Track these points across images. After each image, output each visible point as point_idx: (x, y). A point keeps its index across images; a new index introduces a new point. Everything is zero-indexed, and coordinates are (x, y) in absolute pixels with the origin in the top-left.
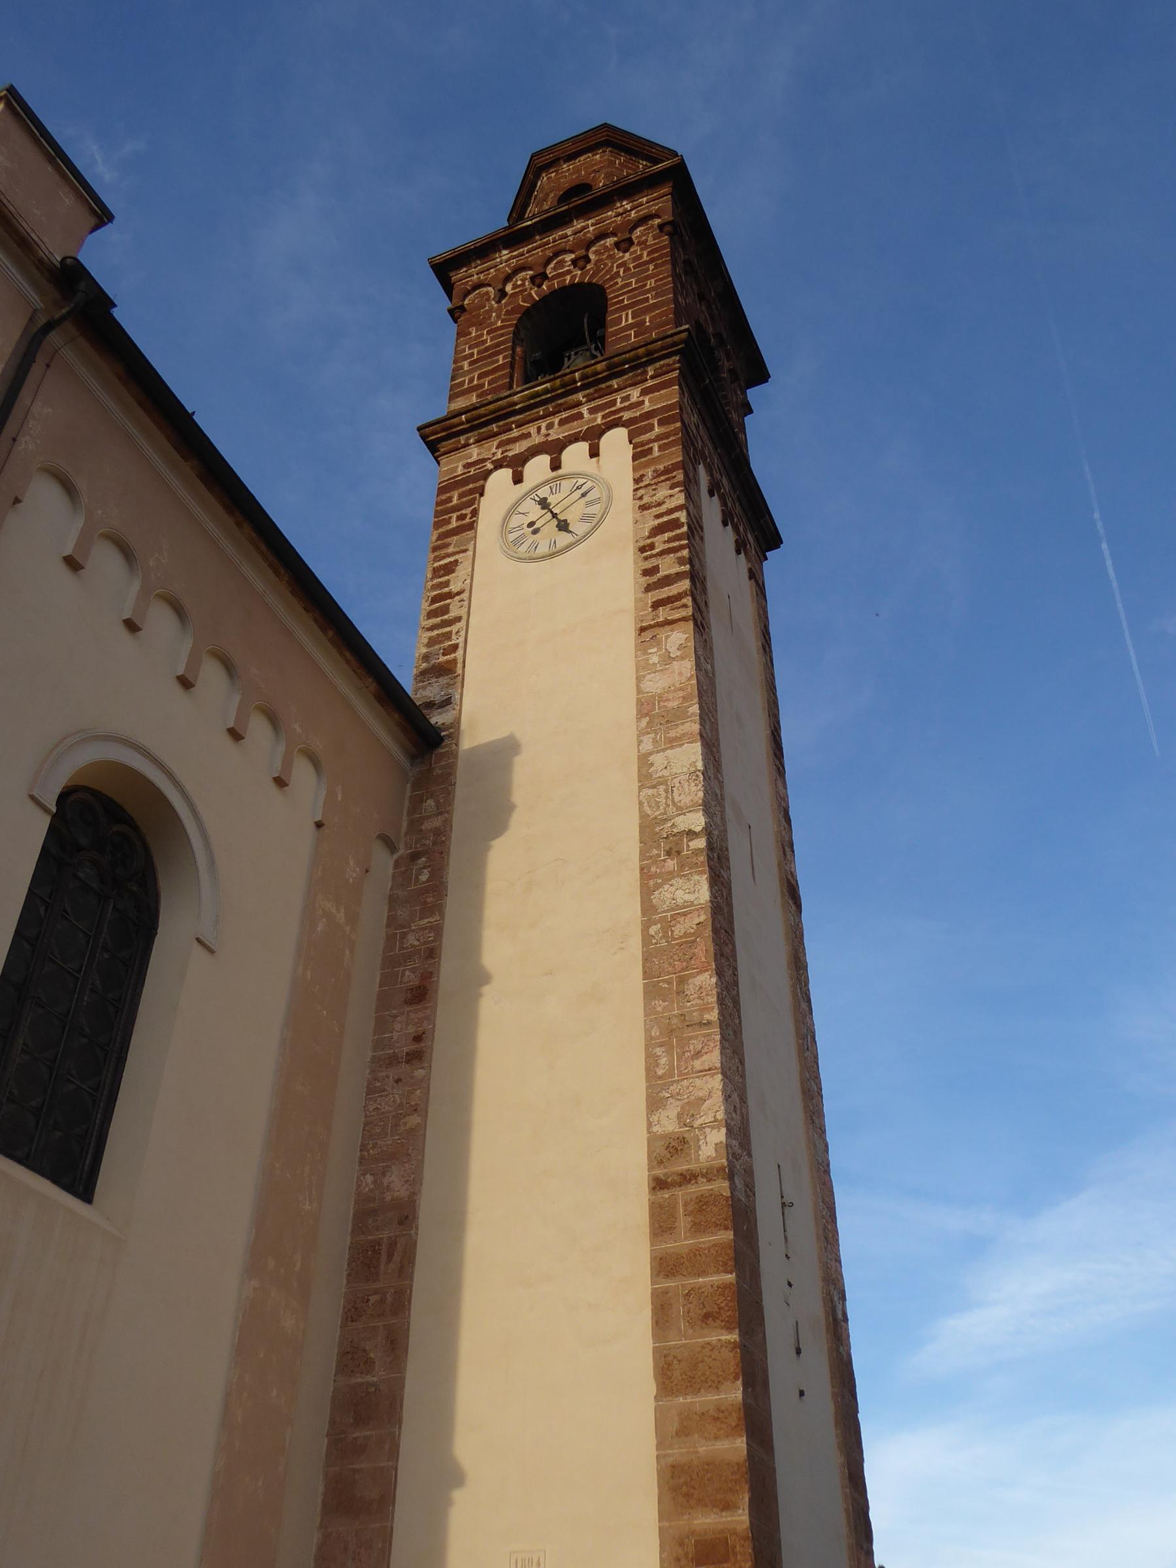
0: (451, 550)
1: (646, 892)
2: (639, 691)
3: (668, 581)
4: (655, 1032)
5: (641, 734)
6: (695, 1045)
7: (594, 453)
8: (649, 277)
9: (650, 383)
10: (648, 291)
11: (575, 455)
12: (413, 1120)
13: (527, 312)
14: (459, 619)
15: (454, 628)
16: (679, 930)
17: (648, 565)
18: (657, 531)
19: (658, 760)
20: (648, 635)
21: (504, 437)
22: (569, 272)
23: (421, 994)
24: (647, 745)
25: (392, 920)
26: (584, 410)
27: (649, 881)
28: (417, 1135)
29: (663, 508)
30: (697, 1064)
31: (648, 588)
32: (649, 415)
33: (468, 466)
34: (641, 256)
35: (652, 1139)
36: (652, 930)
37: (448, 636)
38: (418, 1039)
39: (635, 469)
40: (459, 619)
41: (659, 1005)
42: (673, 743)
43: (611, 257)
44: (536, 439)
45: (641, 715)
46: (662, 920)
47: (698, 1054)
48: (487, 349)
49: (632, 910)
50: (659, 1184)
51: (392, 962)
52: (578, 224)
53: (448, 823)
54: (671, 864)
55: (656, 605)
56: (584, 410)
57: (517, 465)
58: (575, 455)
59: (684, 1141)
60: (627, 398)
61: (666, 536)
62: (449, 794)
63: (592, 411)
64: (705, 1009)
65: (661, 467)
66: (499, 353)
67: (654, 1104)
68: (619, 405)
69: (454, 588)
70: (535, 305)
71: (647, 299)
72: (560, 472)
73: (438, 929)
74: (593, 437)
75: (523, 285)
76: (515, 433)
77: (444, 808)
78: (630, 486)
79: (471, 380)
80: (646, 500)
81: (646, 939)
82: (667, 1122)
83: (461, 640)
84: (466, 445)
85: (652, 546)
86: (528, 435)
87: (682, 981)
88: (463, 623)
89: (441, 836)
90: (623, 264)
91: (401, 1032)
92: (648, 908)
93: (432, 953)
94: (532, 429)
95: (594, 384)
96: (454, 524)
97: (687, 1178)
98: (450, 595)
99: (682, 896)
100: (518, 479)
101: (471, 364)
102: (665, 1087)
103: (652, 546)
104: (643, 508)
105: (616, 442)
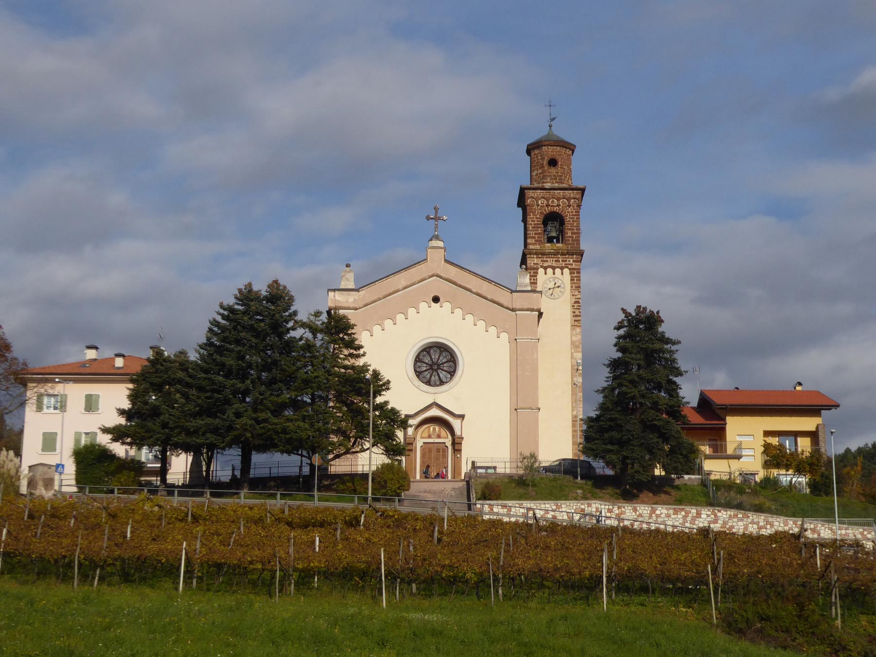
11: (558, 271)
18: (576, 302)
32: (574, 269)
42: (577, 352)
57: (545, 268)
58: (558, 271)
67: (573, 410)
74: (562, 268)
82: (575, 413)
105: (566, 271)
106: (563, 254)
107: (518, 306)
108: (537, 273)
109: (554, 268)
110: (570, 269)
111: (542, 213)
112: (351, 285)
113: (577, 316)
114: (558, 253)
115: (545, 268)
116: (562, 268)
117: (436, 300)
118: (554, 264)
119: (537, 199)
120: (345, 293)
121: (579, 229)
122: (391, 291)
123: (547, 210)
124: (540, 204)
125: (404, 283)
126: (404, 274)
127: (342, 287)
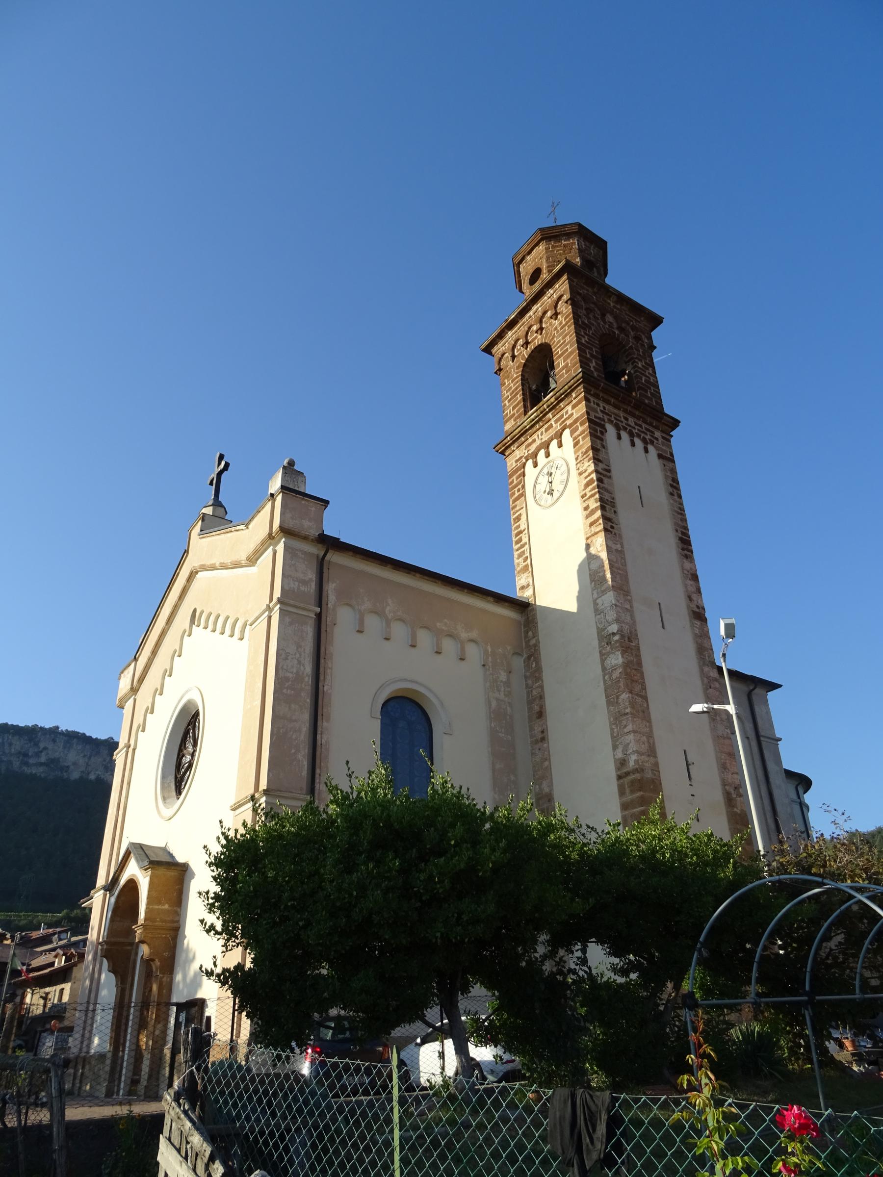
0: (518, 508)
1: (603, 661)
2: (590, 570)
3: (593, 512)
4: (612, 719)
5: (593, 590)
6: (624, 723)
8: (566, 335)
9: (574, 402)
12: (546, 763)
13: (525, 365)
14: (526, 543)
15: (525, 548)
16: (614, 677)
17: (585, 505)
18: (587, 485)
19: (599, 601)
21: (526, 443)
22: (536, 337)
23: (541, 714)
24: (595, 596)
25: (527, 686)
27: (603, 656)
28: (549, 768)
29: (587, 473)
30: (626, 730)
31: (587, 517)
34: (561, 323)
35: (616, 760)
36: (606, 677)
37: (523, 553)
38: (543, 732)
39: (575, 453)
40: (526, 543)
41: (612, 708)
43: (551, 324)
44: (538, 442)
45: (592, 581)
46: (609, 673)
47: (625, 726)
48: (513, 392)
49: (599, 671)
50: (619, 777)
51: (530, 702)
52: (535, 308)
53: (538, 641)
54: (609, 648)
55: (591, 524)
56: (552, 422)
59: (624, 760)
61: (591, 487)
62: (536, 627)
63: (556, 422)
64: (626, 708)
65: (584, 450)
66: (516, 394)
67: (615, 747)
69: (522, 528)
70: (527, 360)
71: (567, 350)
72: (550, 458)
73: (542, 687)
76: (530, 440)
77: (535, 635)
80: (581, 470)
81: (605, 681)
82: (619, 754)
83: (528, 555)
85: (585, 494)
86: (534, 441)
87: (618, 698)
88: (527, 546)
89: (537, 646)
91: (537, 729)
92: (604, 669)
93: (541, 697)
94: (535, 436)
95: (553, 408)
96: (517, 494)
97: (627, 774)
98: (521, 532)
99: (614, 662)
100: (535, 465)
101: (509, 401)
102: (617, 740)
103: (585, 494)
104: (580, 474)
118: (545, 438)
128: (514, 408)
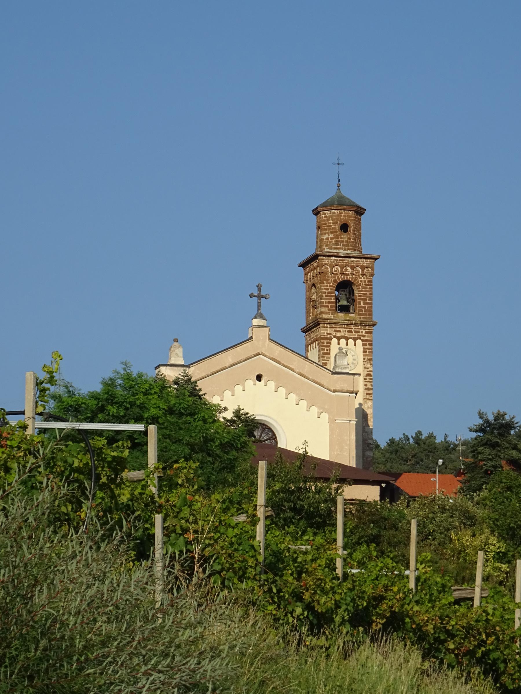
7: (355, 345)
10: (367, 297)
11: (351, 341)
20: (365, 400)
26: (353, 330)
29: (369, 370)
32: (366, 341)
33: (327, 333)
39: (364, 355)
54: (368, 448)
57: (339, 339)
58: (351, 341)
60: (362, 332)
63: (355, 332)
68: (360, 334)
72: (347, 347)
74: (355, 339)
75: (336, 271)
78: (362, 360)
79: (326, 303)
80: (365, 366)
81: (363, 460)
84: (327, 327)
86: (340, 331)
90: (361, 281)
92: (364, 455)
99: (369, 454)
101: (326, 296)
105: (359, 342)
106: (356, 325)
107: (338, 388)
108: (330, 343)
109: (347, 339)
110: (363, 340)
111: (335, 281)
112: (181, 361)
113: (368, 389)
114: (351, 324)
115: (339, 339)
116: (355, 339)
117: (259, 378)
119: (332, 267)
120: (176, 368)
121: (371, 300)
122: (218, 368)
123: (341, 278)
124: (334, 270)
125: (231, 361)
126: (231, 351)
127: (172, 362)
128: (329, 303)
